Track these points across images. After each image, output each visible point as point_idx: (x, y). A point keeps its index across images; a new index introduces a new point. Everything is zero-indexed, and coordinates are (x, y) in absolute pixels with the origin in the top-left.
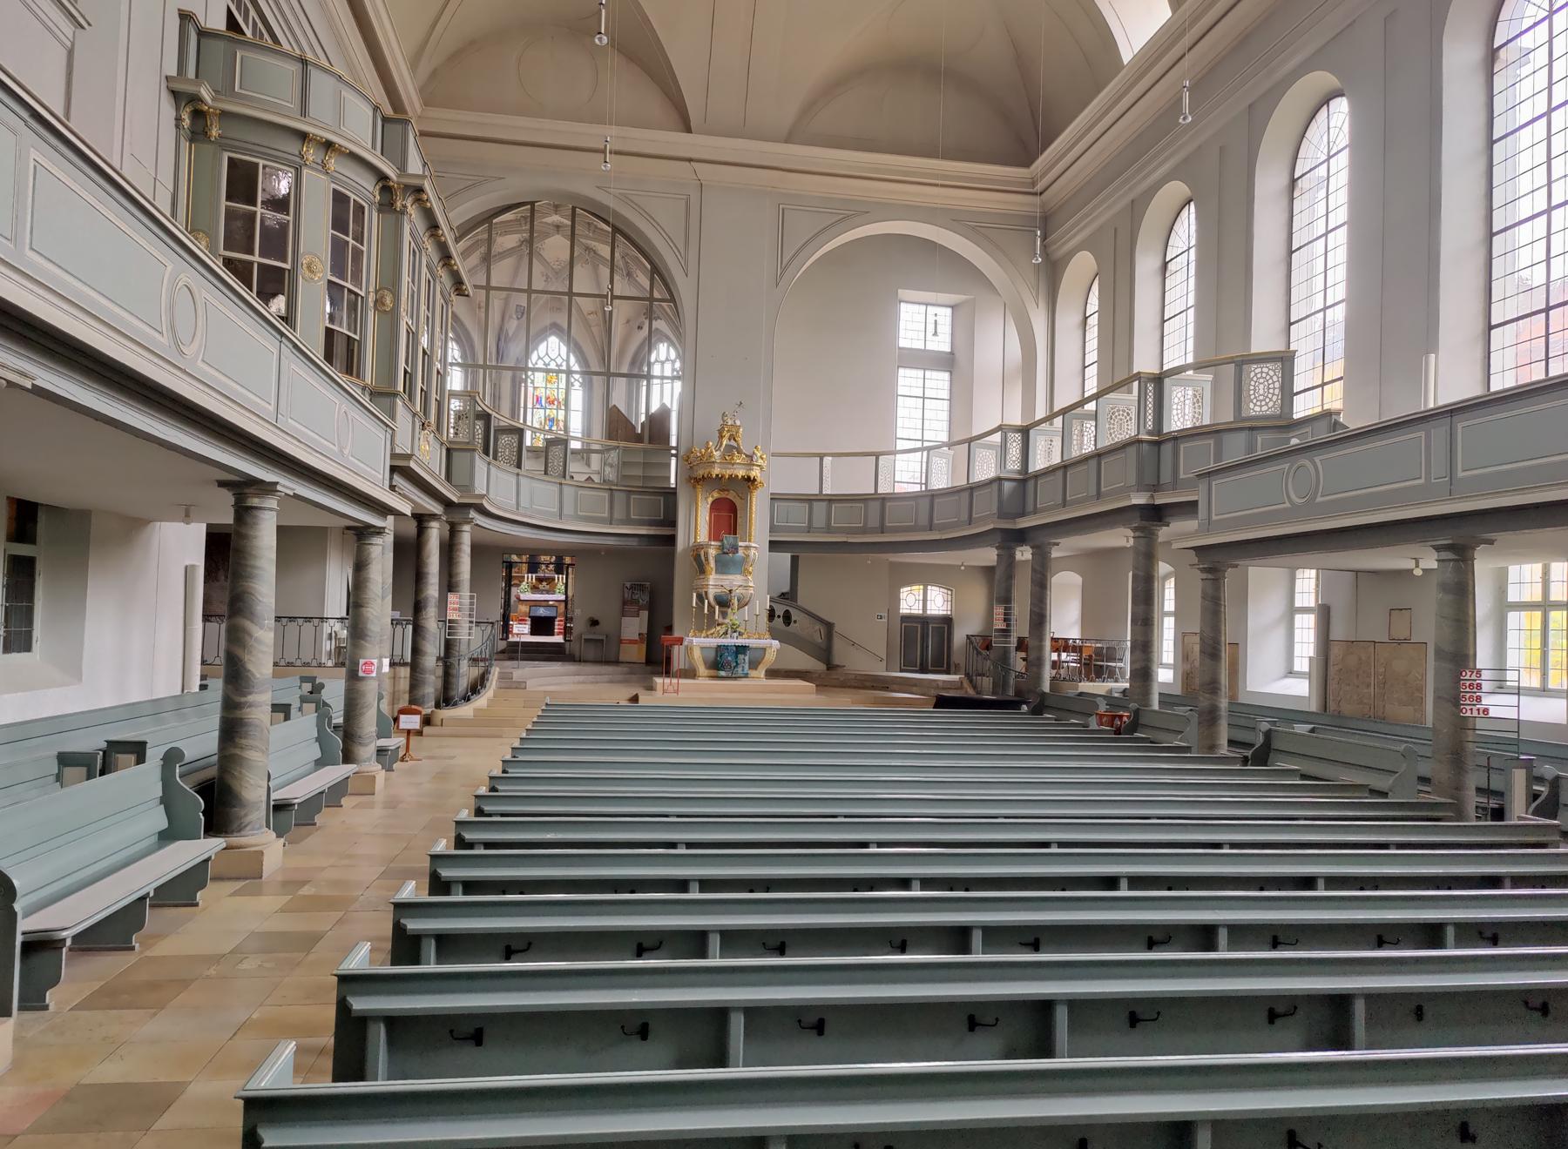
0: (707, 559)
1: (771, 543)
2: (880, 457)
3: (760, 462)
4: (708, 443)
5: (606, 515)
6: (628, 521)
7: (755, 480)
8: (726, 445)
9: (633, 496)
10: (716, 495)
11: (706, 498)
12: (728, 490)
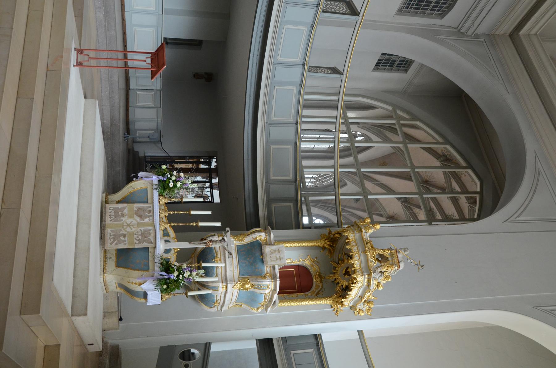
3: (374, 283)
5: (273, 178)
6: (270, 201)
9: (291, 205)
12: (321, 282)
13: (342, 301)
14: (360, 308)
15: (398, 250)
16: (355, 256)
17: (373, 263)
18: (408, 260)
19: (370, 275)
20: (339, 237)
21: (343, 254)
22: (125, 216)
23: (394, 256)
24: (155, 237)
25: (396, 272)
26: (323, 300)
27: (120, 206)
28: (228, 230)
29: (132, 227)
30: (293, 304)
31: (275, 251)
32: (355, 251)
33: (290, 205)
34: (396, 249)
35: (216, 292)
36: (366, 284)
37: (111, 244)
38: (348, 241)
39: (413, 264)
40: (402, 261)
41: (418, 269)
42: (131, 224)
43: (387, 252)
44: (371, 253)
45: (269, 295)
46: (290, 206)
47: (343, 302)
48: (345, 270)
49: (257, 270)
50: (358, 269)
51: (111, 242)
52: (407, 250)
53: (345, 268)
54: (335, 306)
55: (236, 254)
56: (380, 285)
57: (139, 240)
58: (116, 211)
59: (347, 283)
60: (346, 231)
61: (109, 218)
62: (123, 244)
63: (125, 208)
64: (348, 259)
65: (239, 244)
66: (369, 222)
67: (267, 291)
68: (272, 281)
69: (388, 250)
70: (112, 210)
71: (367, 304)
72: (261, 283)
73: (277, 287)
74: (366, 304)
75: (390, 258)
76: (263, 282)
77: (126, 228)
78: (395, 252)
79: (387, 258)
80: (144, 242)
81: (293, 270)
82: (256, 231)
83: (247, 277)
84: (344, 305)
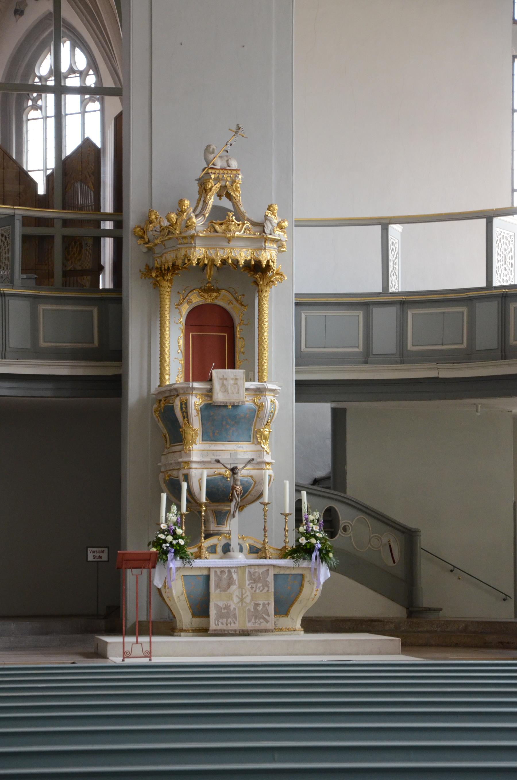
0: (186, 414)
1: (299, 384)
2: (496, 221)
3: (278, 234)
4: (181, 203)
7: (268, 266)
8: (214, 207)
10: (196, 300)
11: (180, 304)
12: (217, 291)
18: (227, 152)
22: (228, 605)
24: (259, 567)
26: (264, 304)
27: (213, 612)
31: (223, 385)
32: (225, 254)
36: (275, 246)
37: (267, 621)
39: (233, 144)
40: (227, 161)
41: (243, 136)
42: (241, 597)
43: (212, 187)
46: (44, 310)
49: (247, 416)
51: (264, 622)
55: (217, 444)
56: (283, 224)
58: (220, 616)
61: (230, 625)
62: (268, 608)
63: (216, 606)
65: (200, 437)
68: (265, 395)
70: (218, 621)
72: (268, 412)
76: (267, 409)
77: (246, 603)
78: (213, 171)
82: (184, 409)
83: (254, 430)
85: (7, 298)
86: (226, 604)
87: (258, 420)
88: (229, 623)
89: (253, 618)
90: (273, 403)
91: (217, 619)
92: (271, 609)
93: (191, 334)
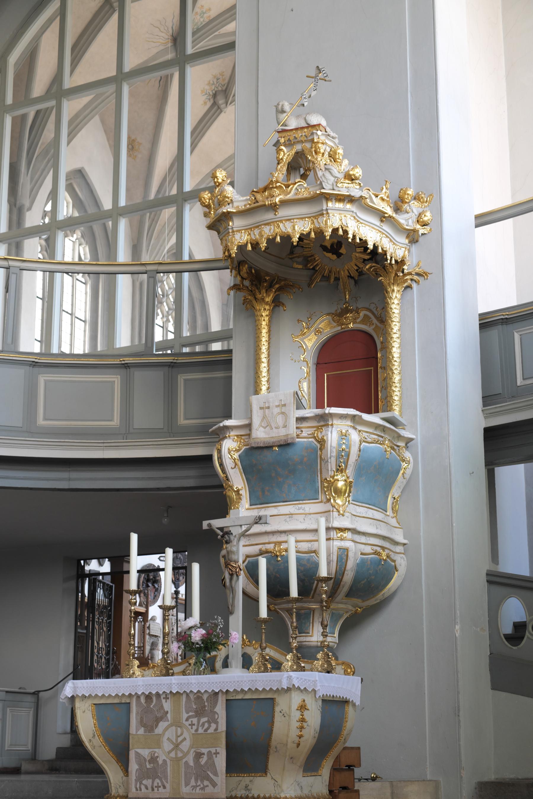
5: (116, 422)
9: (181, 378)
13: (393, 262)
14: (415, 220)
15: (280, 128)
16: (284, 230)
17: (301, 189)
18: (303, 105)
19: (328, 197)
20: (247, 266)
21: (291, 259)
22: (156, 755)
23: (292, 138)
25: (332, 134)
26: (391, 308)
27: (133, 767)
28: (208, 525)
29: (180, 739)
30: (396, 378)
31: (264, 417)
32: (272, 231)
33: (182, 380)
34: (278, 132)
35: (351, 554)
38: (249, 245)
39: (313, 93)
42: (174, 741)
44: (277, 192)
45: (367, 432)
46: (185, 380)
47: (396, 261)
48: (329, 255)
50: (313, 223)
51: (210, 785)
52: (280, 107)
53: (325, 253)
54: (407, 279)
56: (351, 173)
57: (209, 722)
58: (143, 774)
59: (359, 250)
60: (229, 251)
61: (158, 790)
64: (303, 247)
66: (209, 195)
67: (354, 436)
68: (332, 425)
69: (279, 151)
70: (141, 783)
71: (406, 202)
72: (334, 450)
73: (346, 413)
74: (406, 206)
75: (298, 147)
77: (182, 751)
78: (283, 134)
79: (297, 153)
80: (215, 710)
81: (327, 375)
83: (321, 481)
84: (403, 257)
85: (132, 370)
86: (153, 753)
87: (323, 463)
88: (156, 787)
89: (193, 778)
90: (344, 436)
91: (139, 780)
92: (221, 762)
93: (325, 375)
